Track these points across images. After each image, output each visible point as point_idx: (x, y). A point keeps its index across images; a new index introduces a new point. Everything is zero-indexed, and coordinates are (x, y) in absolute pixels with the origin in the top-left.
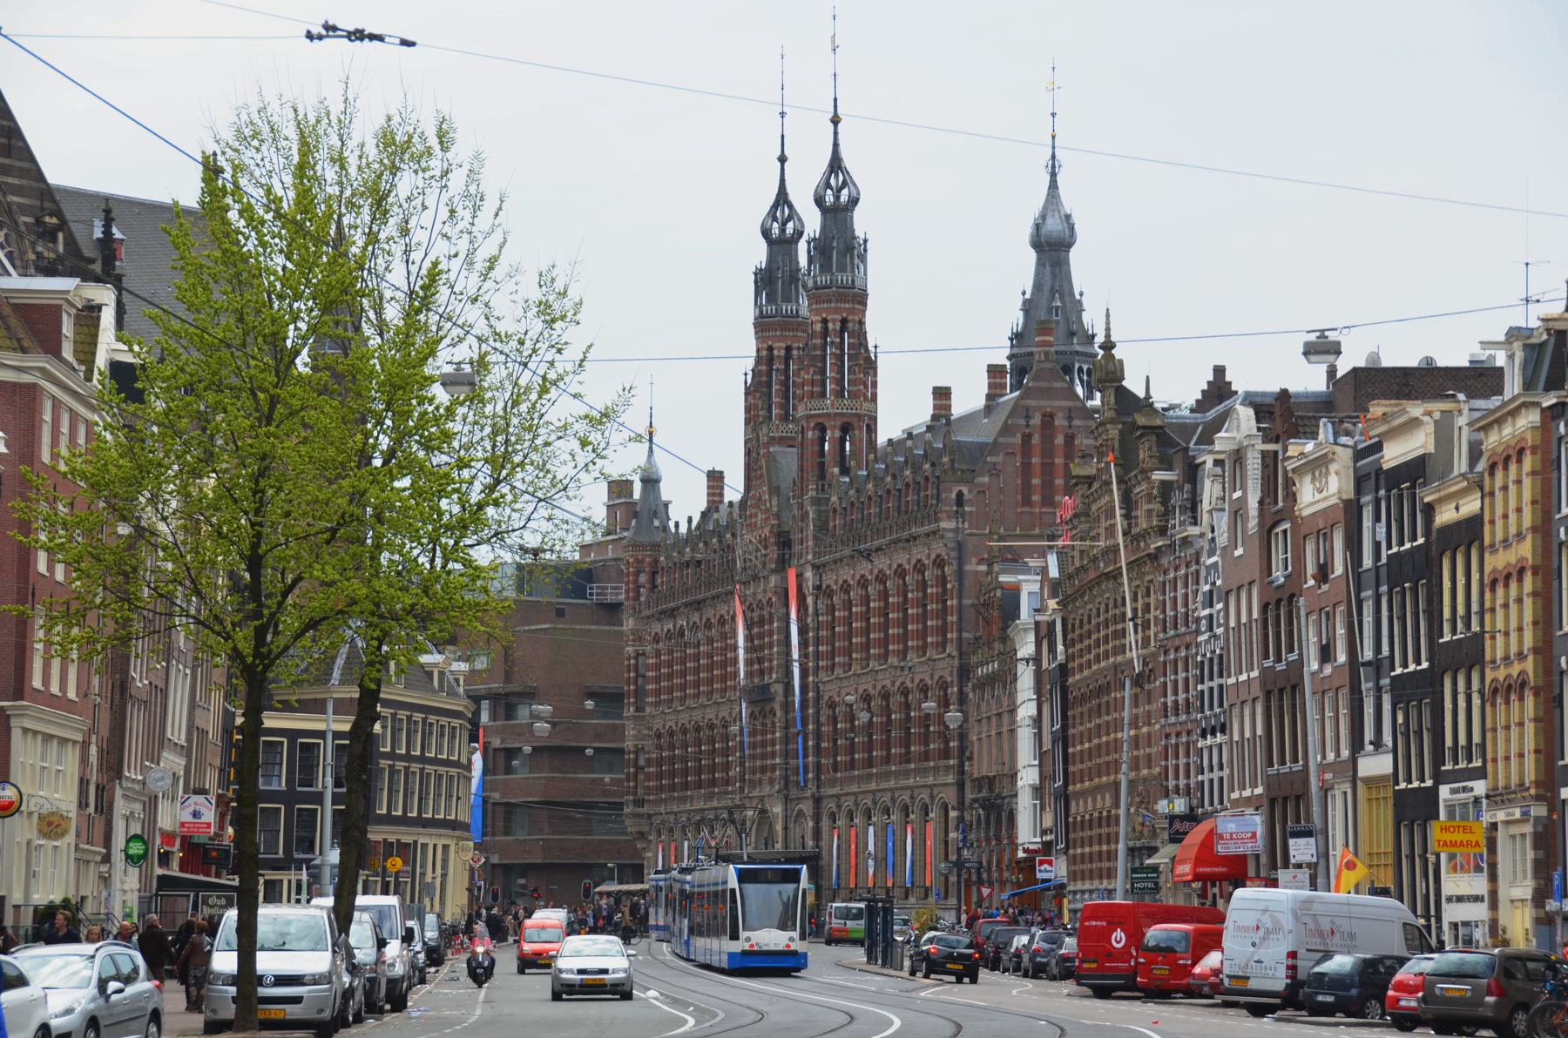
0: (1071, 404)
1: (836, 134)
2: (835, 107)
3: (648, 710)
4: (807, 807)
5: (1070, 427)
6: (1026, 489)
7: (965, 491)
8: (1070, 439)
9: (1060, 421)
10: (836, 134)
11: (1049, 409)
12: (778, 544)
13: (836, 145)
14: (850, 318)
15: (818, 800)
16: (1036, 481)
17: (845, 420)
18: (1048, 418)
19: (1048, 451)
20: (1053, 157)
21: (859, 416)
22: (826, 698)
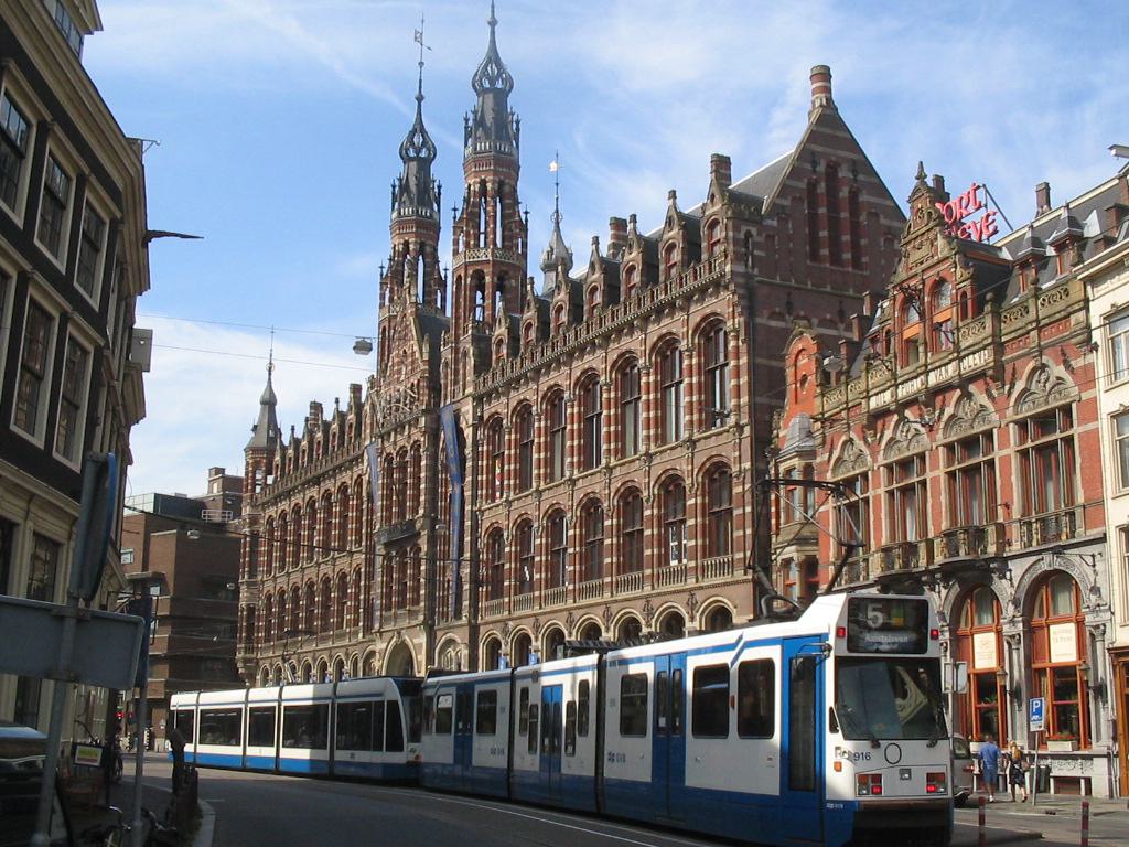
0: (855, 156)
1: (493, 33)
2: (493, 12)
3: (260, 578)
4: (460, 636)
5: (855, 180)
6: (814, 240)
7: (754, 231)
8: (854, 195)
9: (844, 173)
10: (493, 33)
11: (833, 158)
12: (428, 387)
13: (493, 41)
14: (507, 181)
15: (474, 630)
16: (824, 234)
17: (504, 268)
18: (832, 168)
19: (833, 206)
20: (557, 211)
21: (514, 266)
22: (486, 525)
